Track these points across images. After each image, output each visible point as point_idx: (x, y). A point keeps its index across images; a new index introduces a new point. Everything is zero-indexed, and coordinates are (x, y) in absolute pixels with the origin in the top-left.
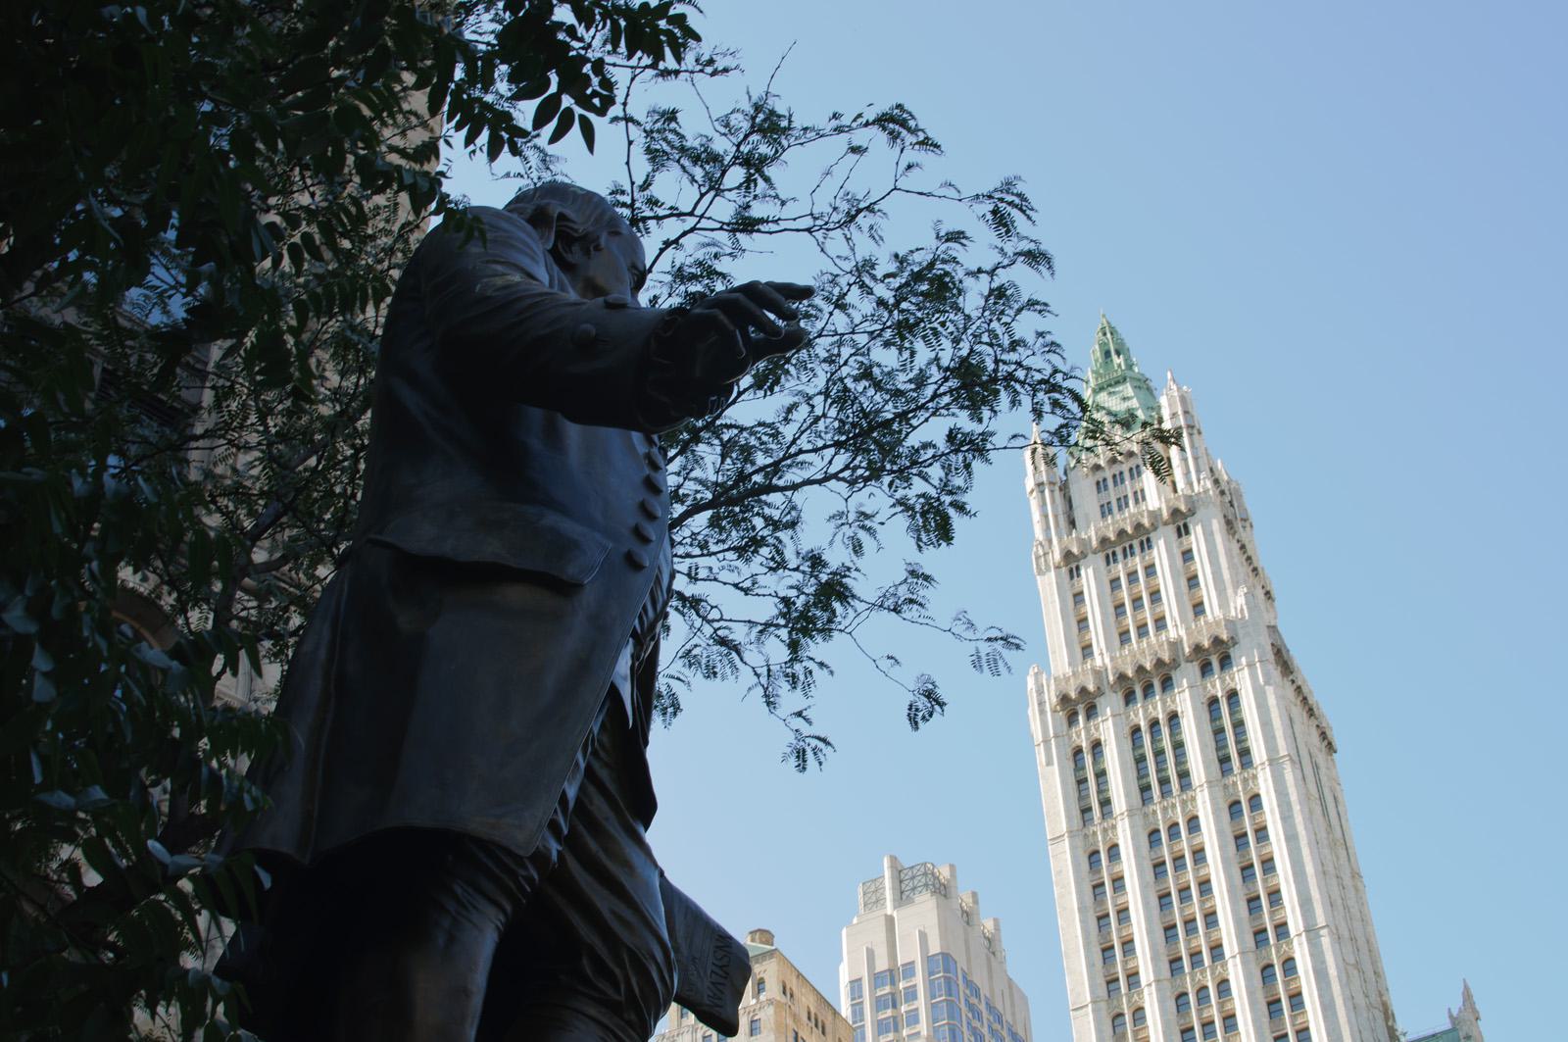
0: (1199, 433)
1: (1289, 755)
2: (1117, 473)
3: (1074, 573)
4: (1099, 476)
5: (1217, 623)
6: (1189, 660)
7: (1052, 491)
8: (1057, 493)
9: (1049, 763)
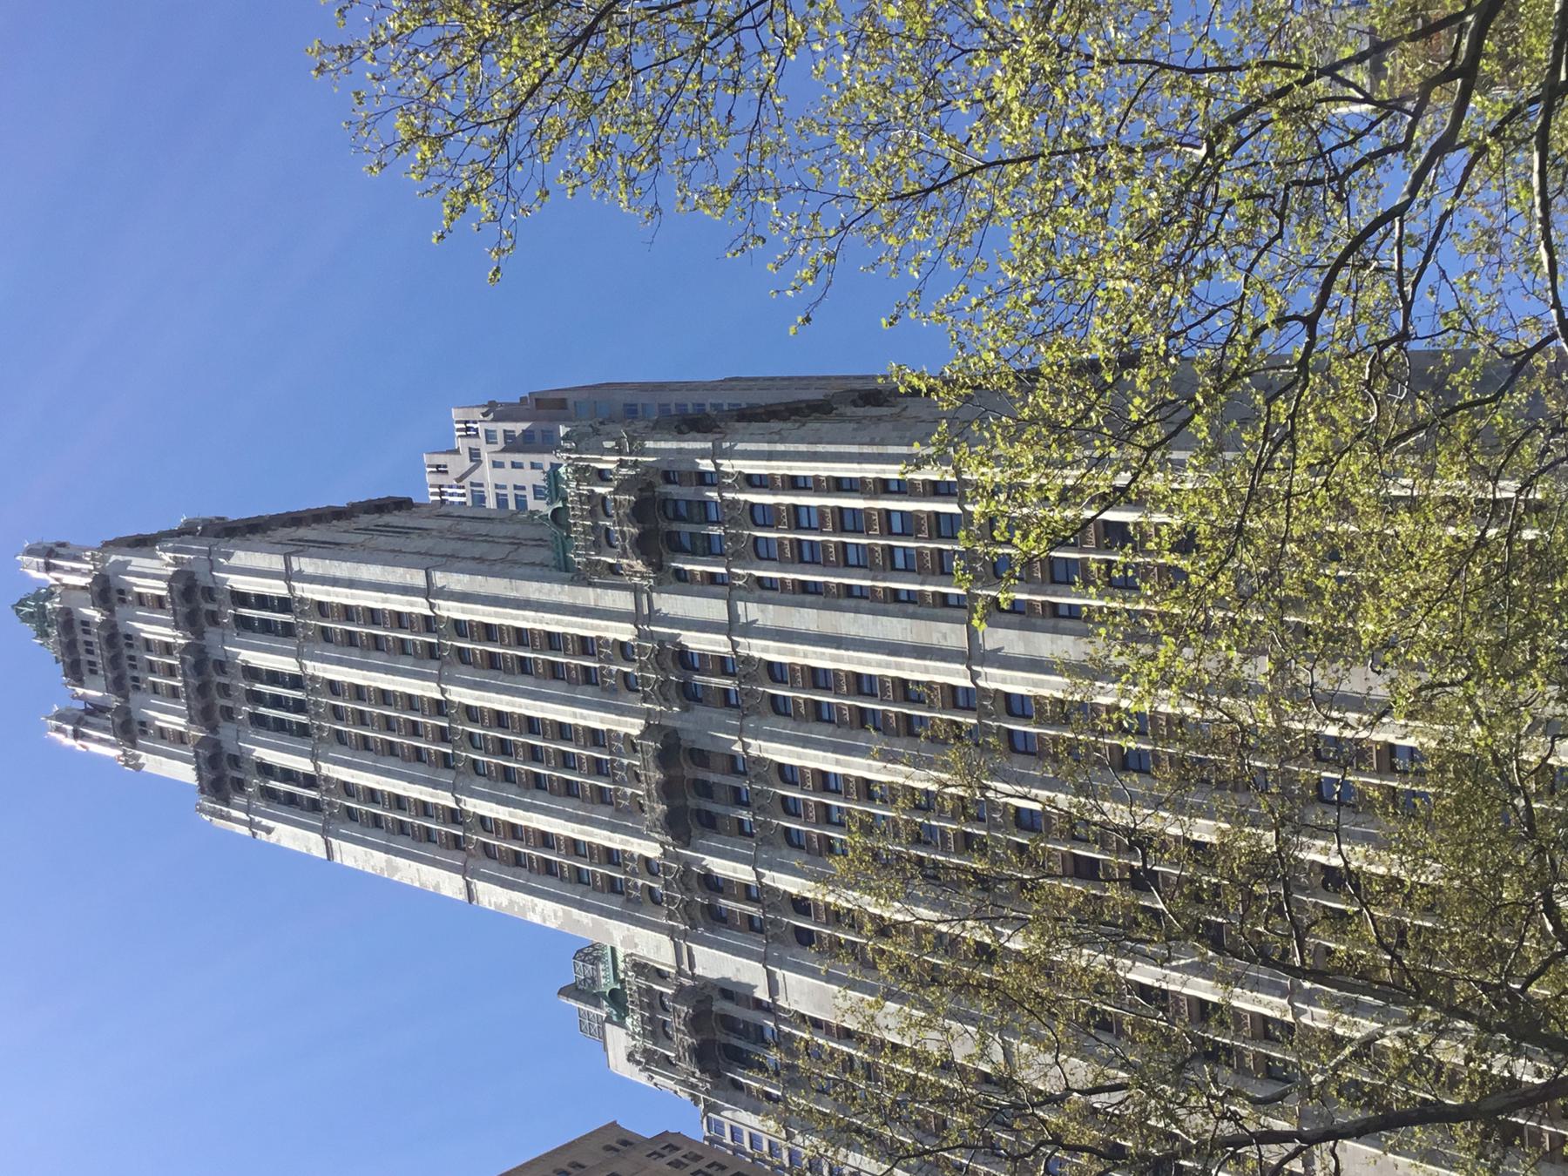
0: (63, 545)
1: (285, 555)
4: (85, 668)
5: (170, 589)
9: (269, 831)
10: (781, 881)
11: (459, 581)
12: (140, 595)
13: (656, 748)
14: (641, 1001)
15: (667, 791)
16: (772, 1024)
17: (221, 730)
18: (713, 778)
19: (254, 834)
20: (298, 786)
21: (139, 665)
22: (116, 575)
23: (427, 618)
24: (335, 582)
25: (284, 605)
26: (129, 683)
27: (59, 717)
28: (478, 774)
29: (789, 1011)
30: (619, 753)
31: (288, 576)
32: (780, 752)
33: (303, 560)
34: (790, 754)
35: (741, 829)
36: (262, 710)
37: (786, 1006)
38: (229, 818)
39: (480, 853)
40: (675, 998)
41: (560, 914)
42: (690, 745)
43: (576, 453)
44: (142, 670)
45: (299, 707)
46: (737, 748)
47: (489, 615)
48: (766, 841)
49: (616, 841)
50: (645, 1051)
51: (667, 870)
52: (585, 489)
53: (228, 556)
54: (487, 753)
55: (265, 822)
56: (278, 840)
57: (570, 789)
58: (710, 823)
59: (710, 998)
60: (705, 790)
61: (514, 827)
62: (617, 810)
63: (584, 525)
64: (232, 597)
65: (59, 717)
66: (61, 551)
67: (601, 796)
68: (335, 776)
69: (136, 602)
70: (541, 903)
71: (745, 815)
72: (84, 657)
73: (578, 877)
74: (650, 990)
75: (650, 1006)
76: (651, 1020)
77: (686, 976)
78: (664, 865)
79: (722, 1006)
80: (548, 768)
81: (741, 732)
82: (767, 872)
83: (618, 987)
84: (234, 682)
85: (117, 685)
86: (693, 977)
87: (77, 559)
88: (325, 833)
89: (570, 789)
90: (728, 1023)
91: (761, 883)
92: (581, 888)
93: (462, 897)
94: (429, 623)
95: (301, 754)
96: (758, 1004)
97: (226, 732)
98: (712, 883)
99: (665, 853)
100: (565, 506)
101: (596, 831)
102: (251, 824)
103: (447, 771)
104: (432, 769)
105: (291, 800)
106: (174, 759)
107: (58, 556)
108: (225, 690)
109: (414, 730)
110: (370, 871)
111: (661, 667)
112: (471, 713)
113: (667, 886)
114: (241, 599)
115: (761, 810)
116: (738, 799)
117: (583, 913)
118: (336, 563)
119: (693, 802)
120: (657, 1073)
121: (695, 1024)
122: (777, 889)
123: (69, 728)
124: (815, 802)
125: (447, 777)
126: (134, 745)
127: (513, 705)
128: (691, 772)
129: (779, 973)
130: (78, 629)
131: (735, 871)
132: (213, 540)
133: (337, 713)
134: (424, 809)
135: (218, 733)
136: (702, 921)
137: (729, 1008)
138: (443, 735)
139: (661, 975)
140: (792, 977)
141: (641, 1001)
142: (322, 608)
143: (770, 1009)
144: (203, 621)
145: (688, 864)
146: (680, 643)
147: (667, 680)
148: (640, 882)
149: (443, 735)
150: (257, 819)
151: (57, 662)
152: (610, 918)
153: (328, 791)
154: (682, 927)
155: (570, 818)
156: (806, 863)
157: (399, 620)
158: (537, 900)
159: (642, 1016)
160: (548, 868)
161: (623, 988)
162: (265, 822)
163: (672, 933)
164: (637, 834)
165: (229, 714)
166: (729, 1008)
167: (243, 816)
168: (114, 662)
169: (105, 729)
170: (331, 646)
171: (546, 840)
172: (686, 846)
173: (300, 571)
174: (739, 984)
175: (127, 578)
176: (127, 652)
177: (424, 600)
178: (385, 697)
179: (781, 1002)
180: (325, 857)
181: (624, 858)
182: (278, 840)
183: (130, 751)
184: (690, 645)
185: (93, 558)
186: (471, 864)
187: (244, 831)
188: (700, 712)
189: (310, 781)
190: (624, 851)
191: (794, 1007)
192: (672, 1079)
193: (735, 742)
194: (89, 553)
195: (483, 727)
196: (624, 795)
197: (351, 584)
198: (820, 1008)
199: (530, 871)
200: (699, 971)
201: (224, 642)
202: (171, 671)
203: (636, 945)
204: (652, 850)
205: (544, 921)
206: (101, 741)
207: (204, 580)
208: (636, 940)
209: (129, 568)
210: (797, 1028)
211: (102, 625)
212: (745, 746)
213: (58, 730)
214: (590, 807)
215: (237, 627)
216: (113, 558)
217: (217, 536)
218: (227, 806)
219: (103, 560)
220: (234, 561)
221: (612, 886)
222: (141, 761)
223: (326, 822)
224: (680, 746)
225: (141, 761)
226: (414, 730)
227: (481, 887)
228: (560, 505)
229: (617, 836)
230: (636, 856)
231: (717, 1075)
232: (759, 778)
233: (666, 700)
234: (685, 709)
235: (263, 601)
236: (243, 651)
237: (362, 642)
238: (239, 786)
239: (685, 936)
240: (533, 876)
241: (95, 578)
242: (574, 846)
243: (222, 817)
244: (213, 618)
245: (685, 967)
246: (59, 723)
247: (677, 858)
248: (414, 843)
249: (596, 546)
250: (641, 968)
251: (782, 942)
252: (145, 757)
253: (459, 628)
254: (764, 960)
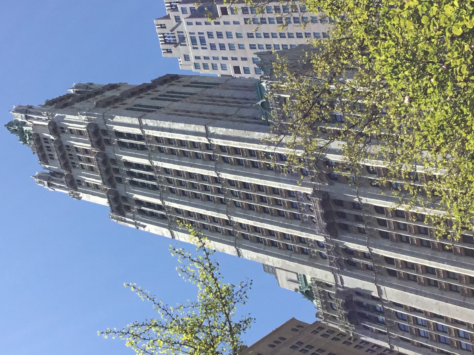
0: (31, 107)
1: (138, 118)
2: (47, 148)
3: (80, 182)
4: (48, 157)
6: (103, 149)
7: (52, 180)
8: (54, 178)
9: (144, 227)
10: (380, 252)
11: (221, 131)
12: (71, 130)
13: (320, 201)
14: (320, 296)
15: (326, 216)
16: (381, 306)
17: (117, 187)
18: (345, 211)
19: (138, 228)
20: (155, 209)
21: (74, 158)
22: (59, 122)
23: (207, 144)
24: (163, 129)
25: (140, 138)
26: (71, 165)
27: (39, 177)
28: (237, 207)
29: (388, 301)
30: (301, 200)
31: (141, 126)
32: (377, 202)
33: (147, 120)
34: (380, 203)
35: (361, 231)
36: (135, 179)
37: (386, 299)
38: (125, 221)
39: (241, 237)
40: (336, 296)
41: (281, 262)
42: (334, 198)
43: (271, 80)
44: (76, 160)
45: (151, 178)
46: (356, 200)
47: (237, 145)
48: (371, 236)
49: (304, 235)
50: (324, 314)
51: (328, 247)
52: (276, 95)
53: (112, 118)
54: (240, 199)
55: (142, 223)
56: (149, 230)
57: (280, 214)
58: (346, 228)
59: (351, 296)
60: (343, 215)
61: (255, 228)
62: (303, 222)
63: (277, 110)
64: (115, 134)
65: (39, 177)
66: (31, 110)
67: (295, 217)
68: (172, 206)
69: (69, 132)
70: (271, 258)
71: (362, 226)
72: (47, 153)
73: (287, 247)
74: (324, 292)
75: (325, 297)
76: (326, 303)
77: (340, 287)
78: (326, 245)
79: (356, 298)
80: (269, 205)
81: (357, 194)
82: (374, 249)
83: (309, 289)
84: (121, 168)
85: (66, 166)
86: (343, 287)
87: (40, 114)
88: (169, 228)
89: (280, 214)
90: (360, 304)
91: (371, 252)
92: (289, 252)
93: (235, 254)
94: (208, 147)
95: (155, 197)
96: (373, 298)
97: (120, 188)
99: (326, 240)
100: (267, 101)
101: (294, 231)
102: (135, 224)
103: (222, 205)
104: (216, 205)
105: (152, 214)
106: (95, 195)
107: (30, 113)
108: (117, 171)
109: (206, 189)
110: (192, 243)
111: (318, 168)
112: (231, 183)
113: (328, 253)
114: (120, 134)
115: (369, 224)
116: (359, 219)
117: (292, 263)
118: (162, 122)
119: (337, 221)
120: (330, 322)
121: (346, 305)
122: (379, 255)
123: (46, 182)
124: (393, 222)
125: (223, 208)
126: (77, 190)
127: (251, 181)
128: (335, 208)
129: (382, 287)
130: (43, 141)
131: (359, 247)
132: (103, 110)
133: (170, 181)
134: (213, 220)
135: (116, 188)
136: (345, 266)
137: (360, 299)
138: (219, 191)
139: (329, 286)
140: (388, 289)
141: (320, 296)
142: (157, 139)
143: (379, 300)
144: (104, 143)
145: (337, 244)
146: (326, 158)
147: (322, 173)
148: (316, 251)
149: (219, 191)
150: (138, 222)
151: (34, 153)
152: (304, 264)
153: (169, 212)
154: (337, 269)
155: (282, 226)
156: (391, 245)
157: (194, 145)
158: (269, 257)
159: (321, 301)
160: (273, 244)
161: (311, 290)
162: (142, 223)
163: (332, 271)
164: (313, 232)
165: (120, 180)
166: (360, 299)
167: (132, 221)
168: (63, 157)
169: (62, 182)
170: (162, 154)
171: (271, 233)
172: (336, 237)
173: (146, 125)
174: (364, 290)
175: (65, 123)
176: (68, 152)
177: (206, 138)
178: (190, 175)
179: (384, 297)
180: (171, 237)
181: (308, 241)
182: (149, 230)
183: (75, 192)
184: (331, 159)
185: (47, 115)
186: (238, 242)
187: (133, 226)
188: (338, 185)
189: (160, 207)
190: (307, 239)
191: (390, 300)
192: (337, 325)
193: (355, 198)
194: (45, 113)
195: (237, 188)
196: (306, 217)
197: (171, 130)
198: (402, 301)
199: (265, 245)
200: (345, 285)
201: (114, 152)
202: (89, 160)
203: (316, 275)
204: (321, 239)
205: (274, 264)
206: (60, 187)
207: (102, 127)
208: (316, 273)
209: (65, 119)
210: (391, 307)
211: (56, 142)
212: (360, 199)
213: (40, 182)
214: (290, 221)
215: (119, 145)
216: (57, 115)
217: (104, 107)
218: (124, 217)
219: (53, 116)
220: (115, 120)
221: (303, 251)
222: (80, 196)
223: (169, 224)
224: (330, 199)
225: (80, 196)
226: (206, 189)
227: (243, 251)
228: (265, 100)
229: (304, 233)
230: (313, 240)
231: (357, 324)
232: (367, 211)
233: (322, 180)
234: (331, 184)
235: (130, 136)
236: (124, 156)
237: (178, 153)
238: (128, 209)
239: (338, 272)
240: (267, 247)
241: (50, 123)
242: (284, 236)
243: (122, 221)
244: (108, 142)
245: (339, 283)
246: (40, 180)
247: (332, 242)
248: (210, 233)
250: (319, 283)
251: (382, 275)
252: (81, 195)
253: (222, 149)
254: (375, 282)
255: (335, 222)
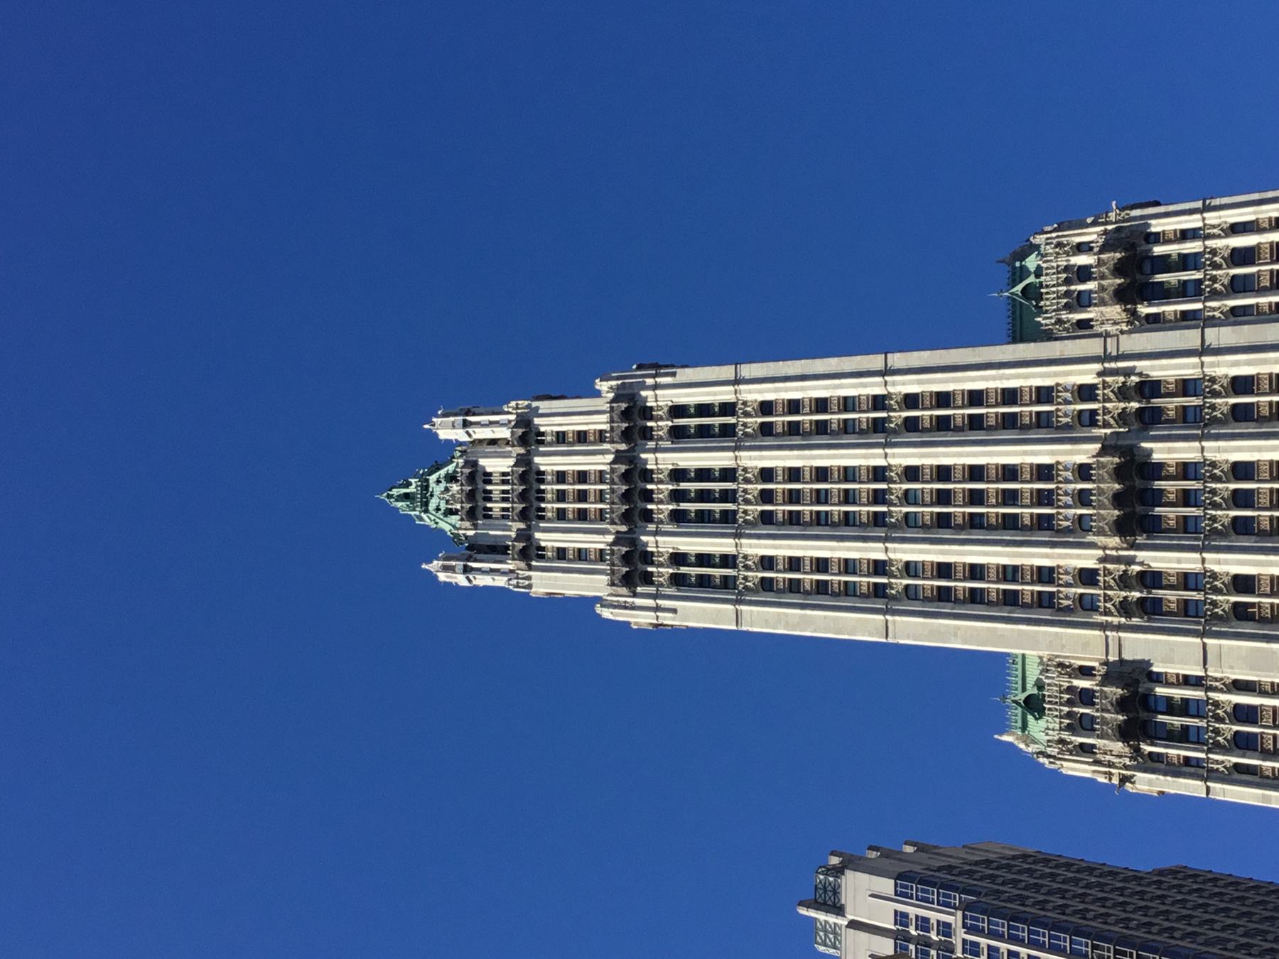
98: (1151, 579)
249: (1068, 307)
255: (1134, 512)
